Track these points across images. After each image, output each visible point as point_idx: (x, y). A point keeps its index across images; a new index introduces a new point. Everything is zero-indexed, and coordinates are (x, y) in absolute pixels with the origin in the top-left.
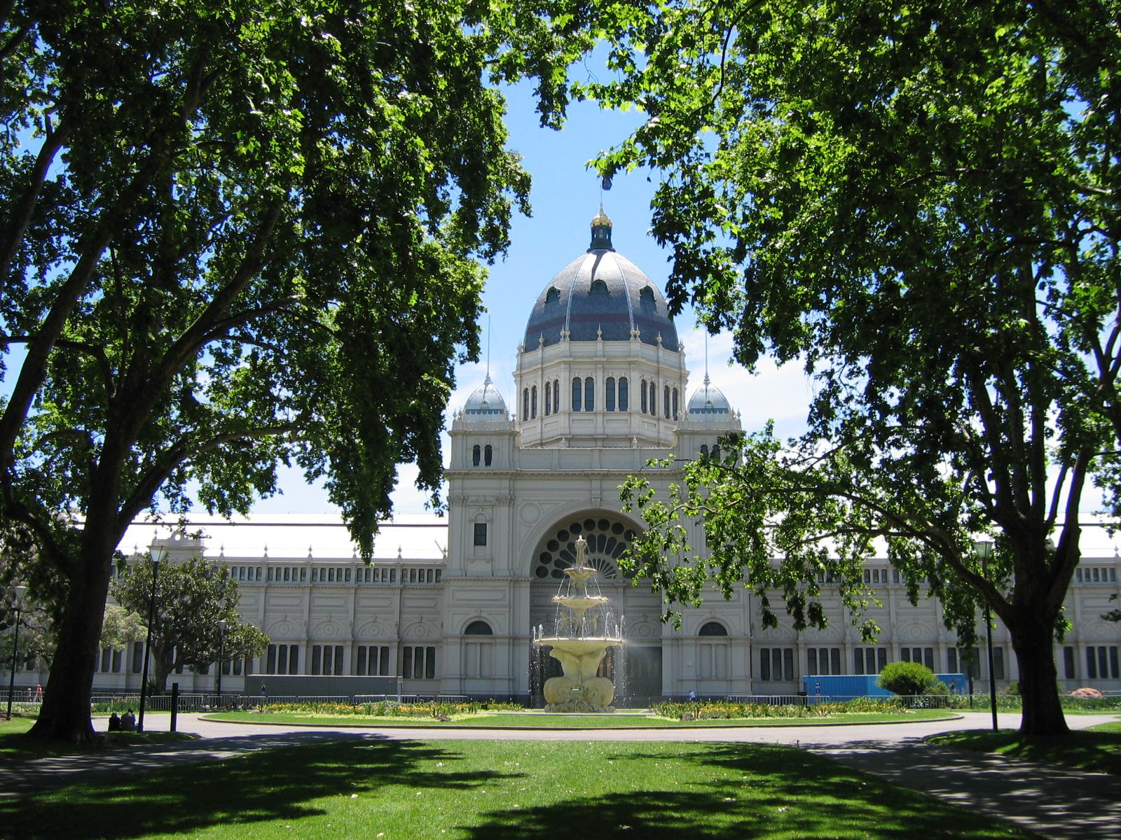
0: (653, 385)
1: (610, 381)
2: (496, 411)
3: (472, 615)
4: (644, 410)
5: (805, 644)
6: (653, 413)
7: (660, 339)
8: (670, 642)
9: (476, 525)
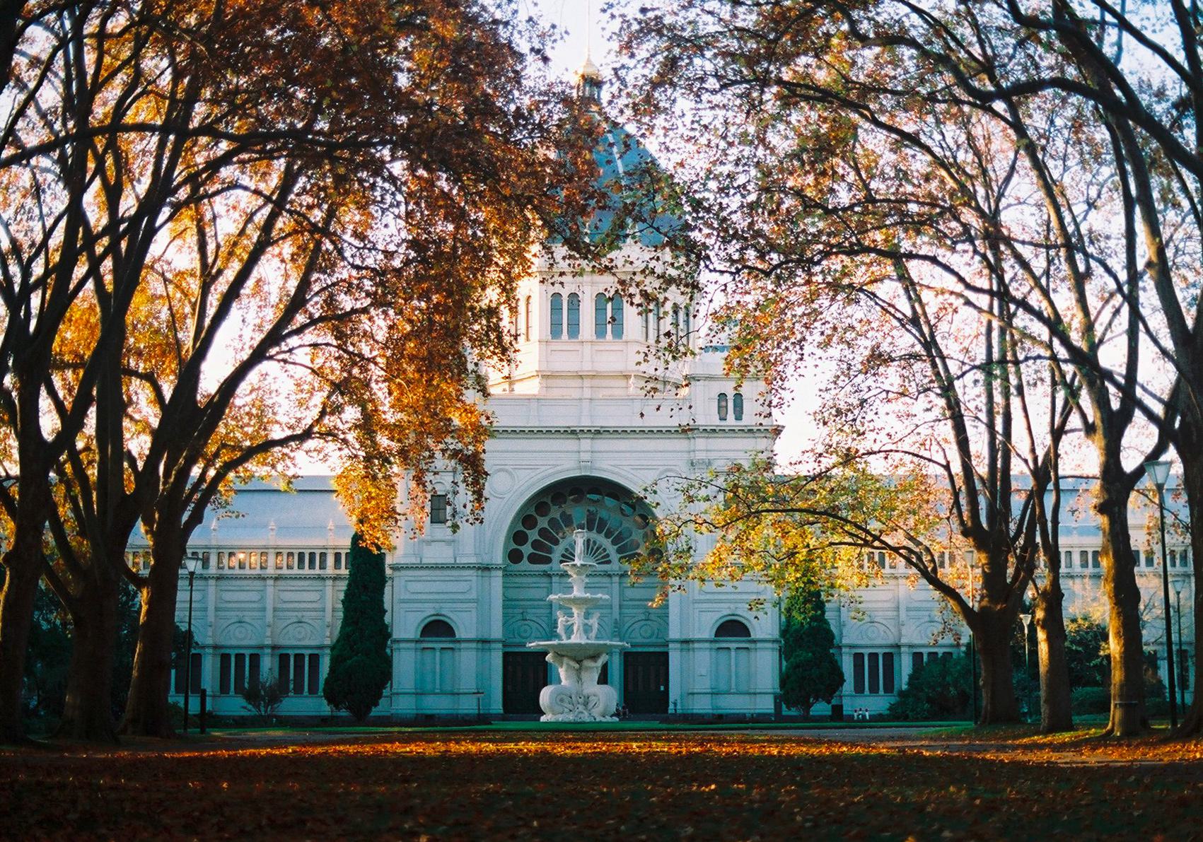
3: (427, 612)
5: (851, 647)
8: (678, 645)
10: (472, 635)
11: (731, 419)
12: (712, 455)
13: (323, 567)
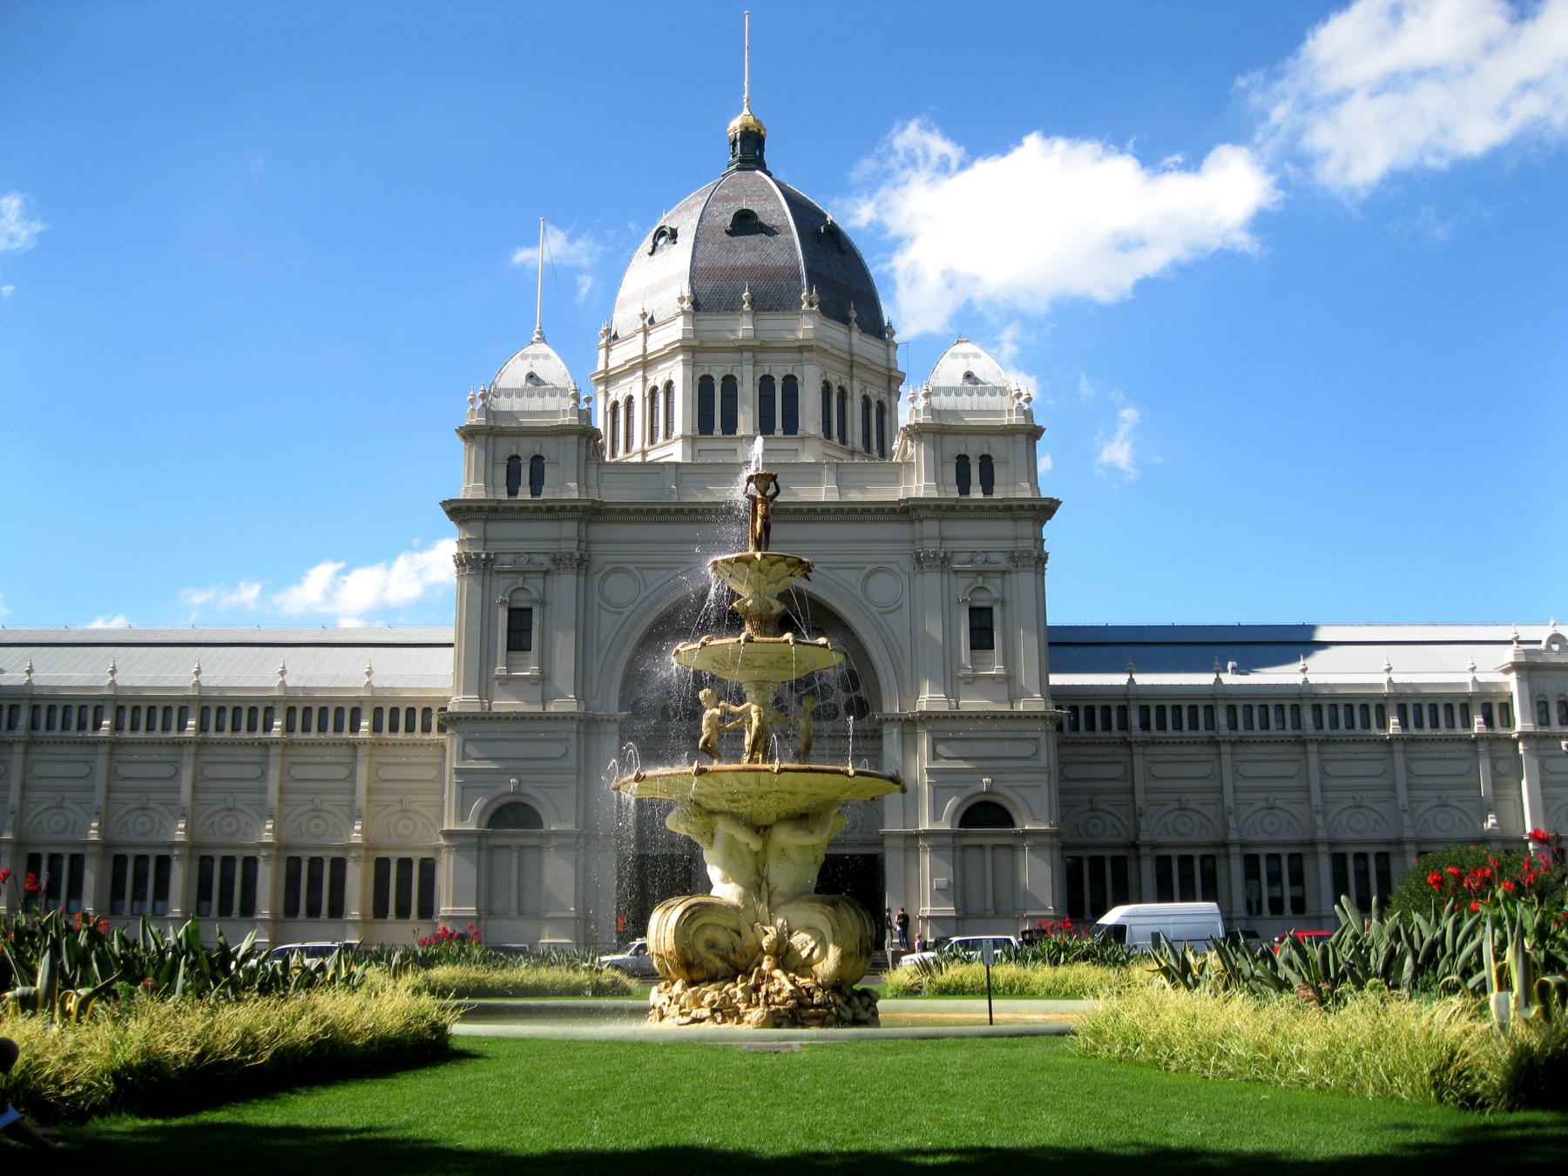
0: (842, 390)
1: (766, 383)
4: (828, 435)
5: (1154, 846)
6: (843, 440)
7: (853, 314)
9: (510, 610)
12: (950, 546)
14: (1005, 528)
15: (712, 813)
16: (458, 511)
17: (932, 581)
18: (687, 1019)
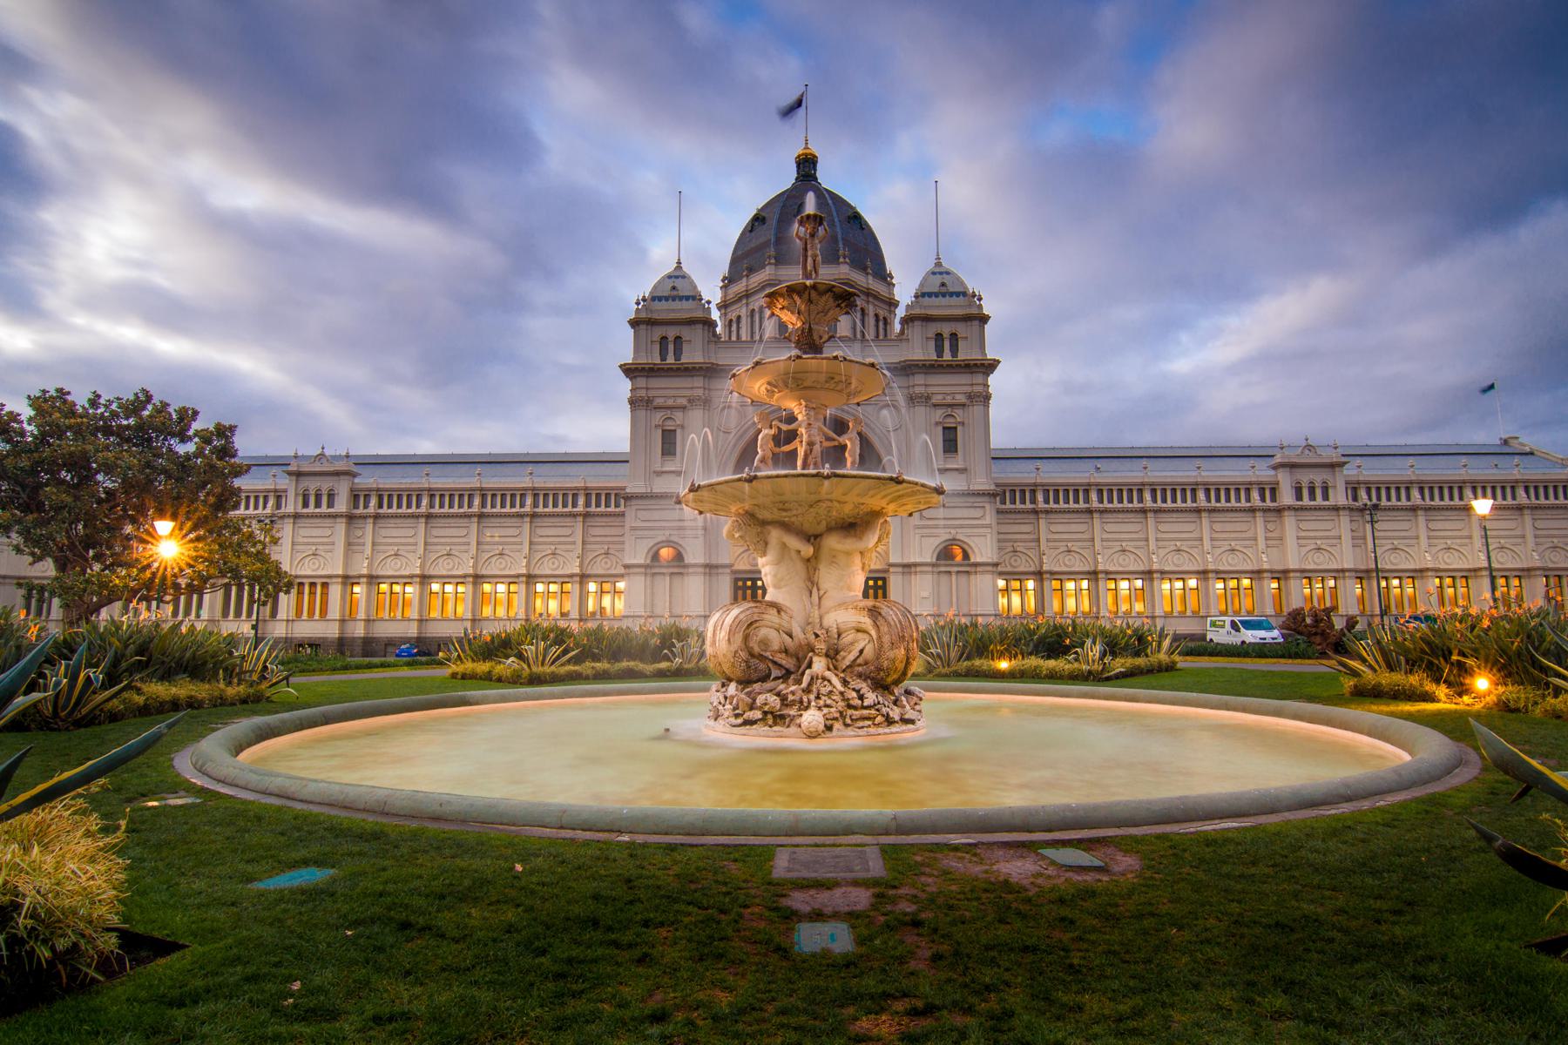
2: (687, 298)
10: (701, 560)
11: (947, 356)
12: (930, 390)
13: (575, 505)
14: (964, 379)
15: (764, 523)
16: (629, 371)
17: (921, 411)
18: (740, 721)
